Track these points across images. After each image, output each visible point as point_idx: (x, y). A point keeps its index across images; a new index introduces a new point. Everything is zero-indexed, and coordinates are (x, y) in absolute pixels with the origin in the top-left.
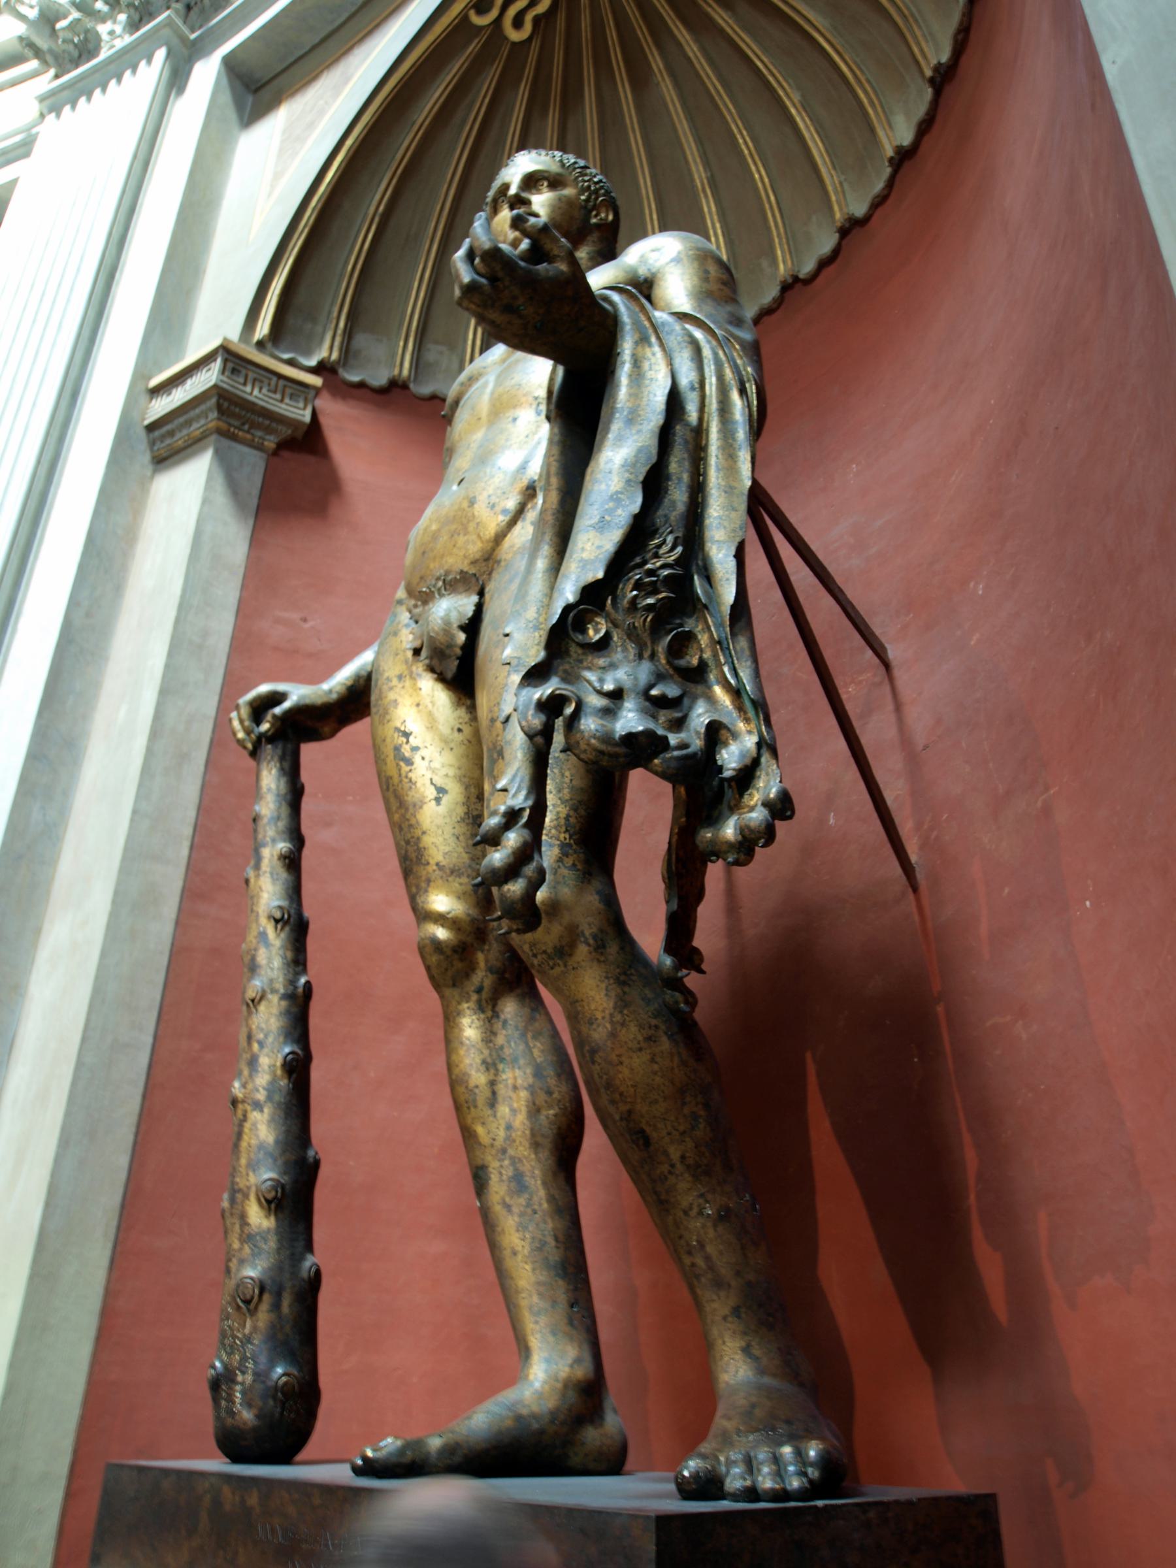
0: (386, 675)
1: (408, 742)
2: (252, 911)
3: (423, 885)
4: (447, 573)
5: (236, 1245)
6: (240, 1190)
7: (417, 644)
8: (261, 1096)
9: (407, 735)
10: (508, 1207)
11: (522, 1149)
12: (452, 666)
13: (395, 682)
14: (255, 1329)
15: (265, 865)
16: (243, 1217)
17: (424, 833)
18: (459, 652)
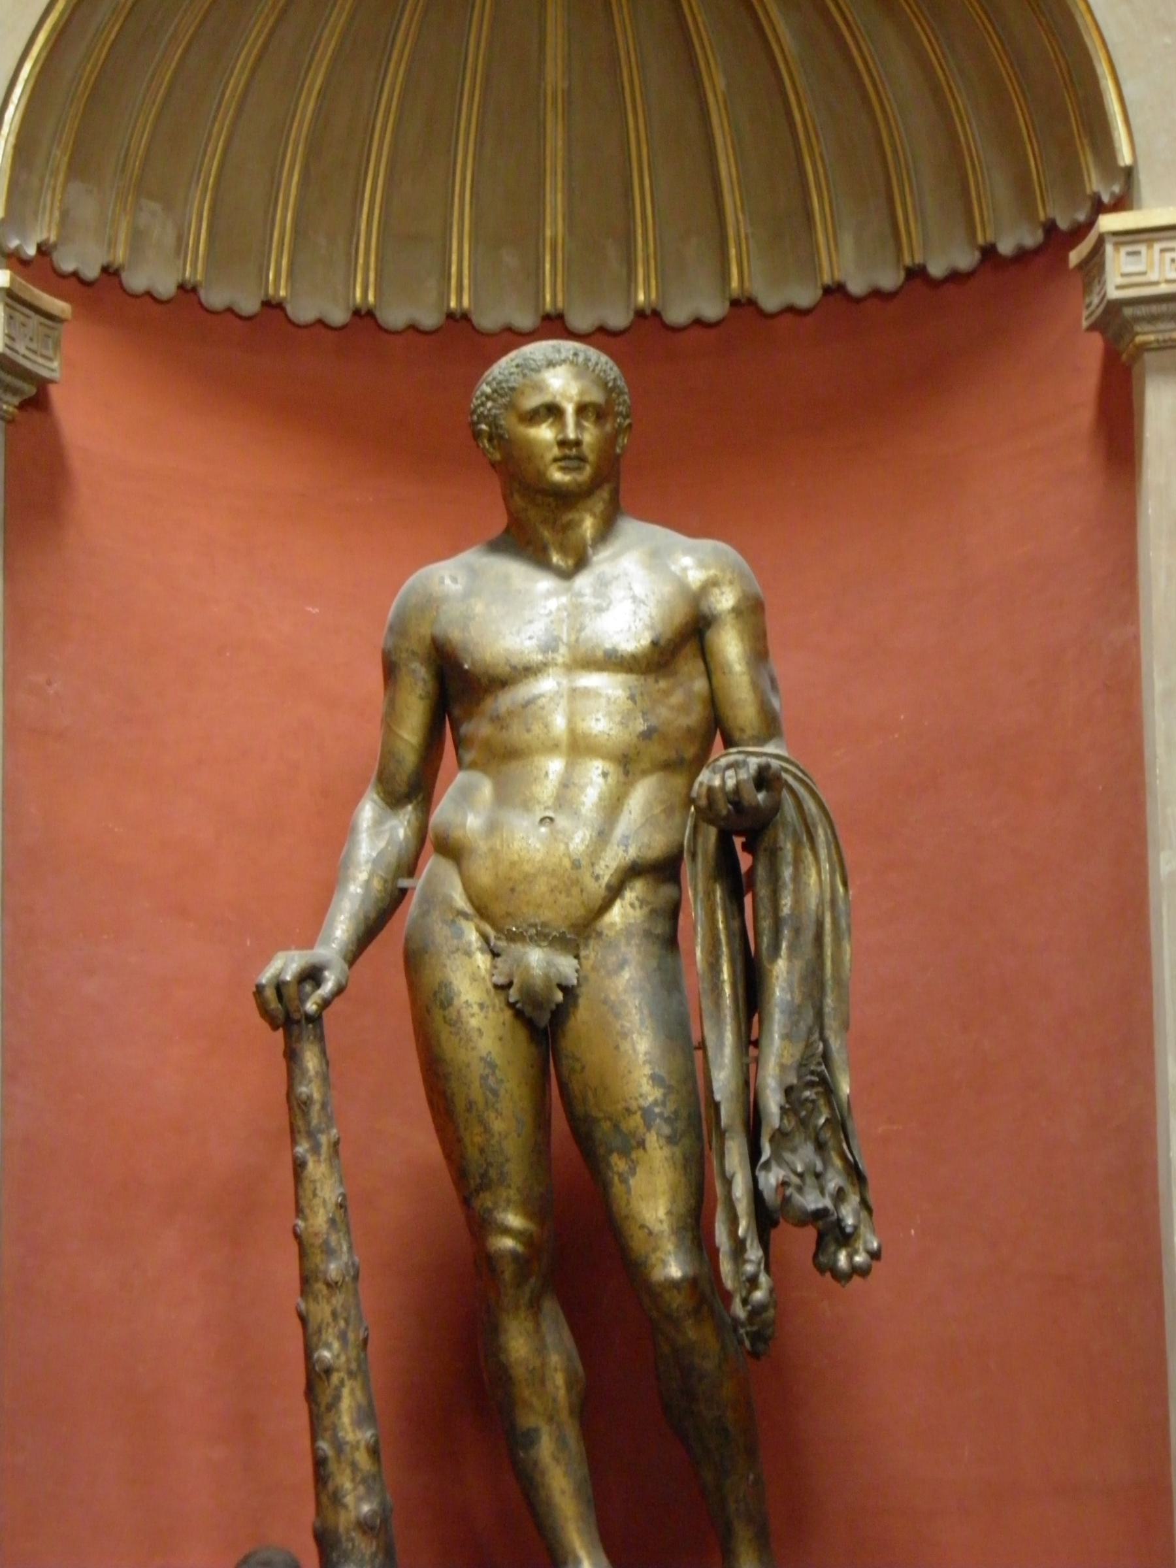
0: (463, 998)
1: (494, 1073)
2: (315, 1195)
3: (503, 1204)
4: (544, 925)
5: (348, 1485)
6: (347, 1443)
7: (501, 980)
8: (354, 1366)
9: (492, 1066)
10: (557, 1460)
11: (564, 1415)
12: (544, 1020)
13: (476, 1009)
14: (378, 1546)
15: (324, 1150)
16: (354, 1466)
17: (507, 1160)
18: (554, 1007)
